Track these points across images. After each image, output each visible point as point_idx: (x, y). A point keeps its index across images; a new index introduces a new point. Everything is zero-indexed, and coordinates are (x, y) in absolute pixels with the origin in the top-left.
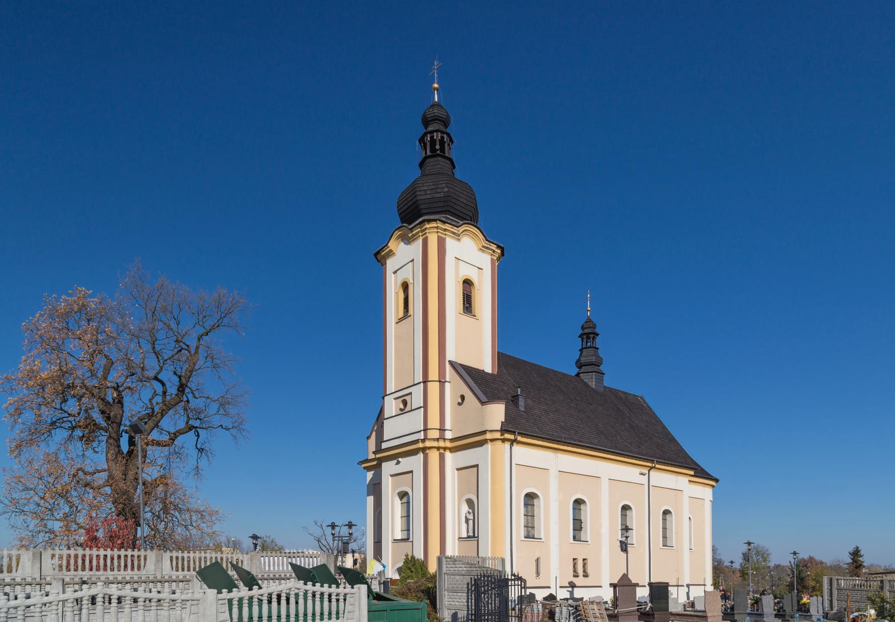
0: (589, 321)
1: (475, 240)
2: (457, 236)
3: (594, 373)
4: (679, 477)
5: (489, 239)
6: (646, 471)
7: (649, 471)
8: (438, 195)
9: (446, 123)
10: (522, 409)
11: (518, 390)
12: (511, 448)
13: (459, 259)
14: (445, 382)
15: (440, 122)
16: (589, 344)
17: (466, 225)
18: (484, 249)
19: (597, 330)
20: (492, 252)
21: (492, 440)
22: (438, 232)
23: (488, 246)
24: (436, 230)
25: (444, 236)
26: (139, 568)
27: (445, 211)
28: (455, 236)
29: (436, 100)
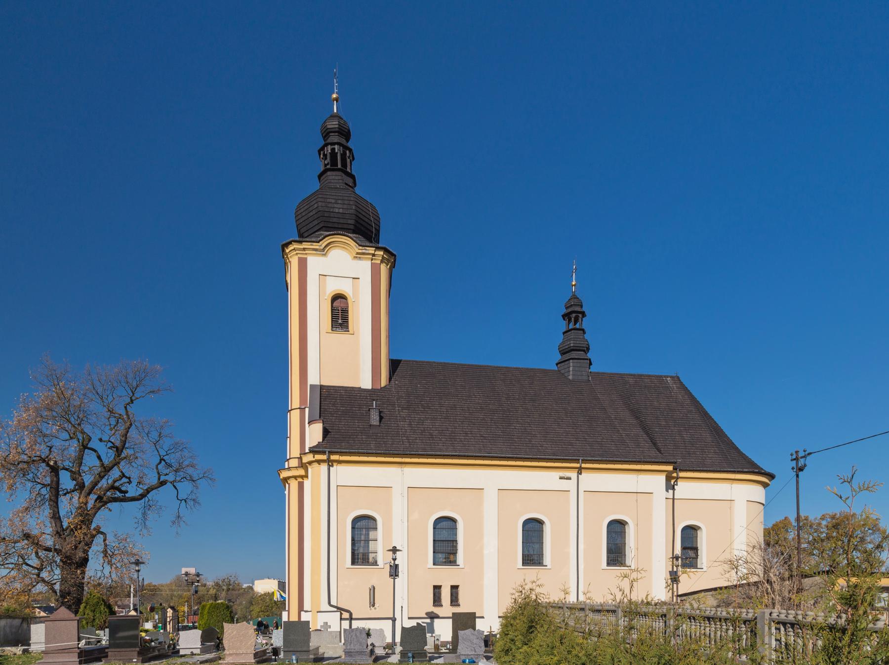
0: (574, 297)
1: (347, 249)
2: (323, 252)
3: (571, 361)
5: (362, 244)
6: (573, 475)
7: (580, 473)
8: (311, 214)
9: (345, 133)
10: (375, 424)
11: (373, 403)
13: (326, 276)
14: (305, 408)
15: (333, 134)
16: (578, 326)
17: (329, 237)
18: (358, 256)
19: (584, 309)
20: (371, 256)
21: (310, 463)
22: (297, 254)
23: (364, 251)
24: (295, 253)
25: (305, 256)
27: (322, 228)
29: (335, 111)
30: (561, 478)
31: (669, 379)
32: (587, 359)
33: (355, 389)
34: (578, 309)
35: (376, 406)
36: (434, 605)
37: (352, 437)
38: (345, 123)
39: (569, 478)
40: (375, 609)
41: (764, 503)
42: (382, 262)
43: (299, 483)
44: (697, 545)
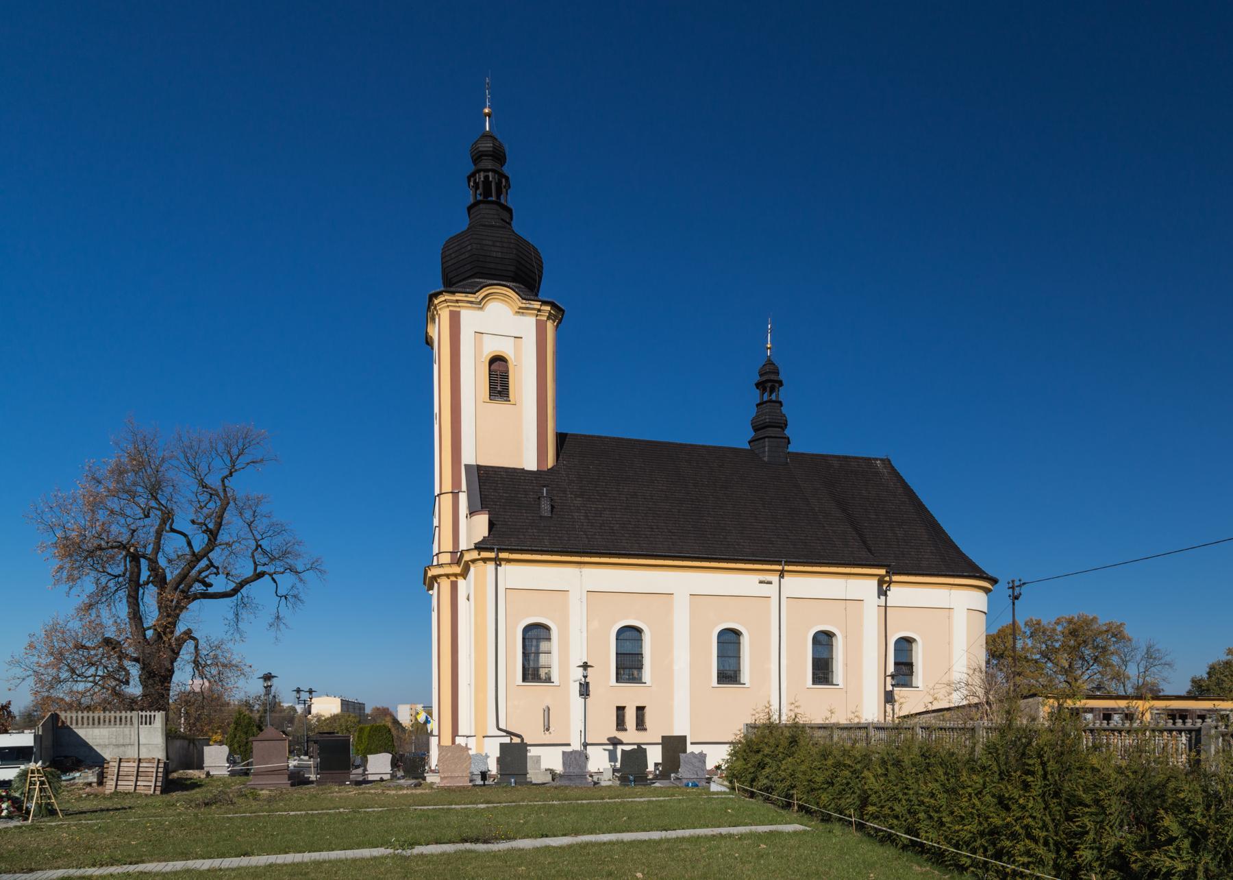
0: (770, 362)
2: (480, 305)
3: (767, 439)
4: (849, 581)
6: (774, 578)
8: (463, 257)
9: (499, 156)
12: (496, 569)
16: (774, 397)
18: (521, 311)
19: (781, 377)
21: (474, 561)
23: (528, 306)
24: (446, 305)
25: (458, 309)
26: (150, 724)
27: (475, 274)
28: (474, 305)
29: (488, 129)
30: (761, 582)
31: (878, 462)
32: (785, 438)
33: (518, 471)
34: (773, 377)
35: (547, 494)
36: (618, 729)
37: (521, 530)
38: (500, 144)
39: (770, 583)
40: (550, 733)
41: (986, 611)
42: (548, 318)
43: (452, 582)
44: (912, 659)
